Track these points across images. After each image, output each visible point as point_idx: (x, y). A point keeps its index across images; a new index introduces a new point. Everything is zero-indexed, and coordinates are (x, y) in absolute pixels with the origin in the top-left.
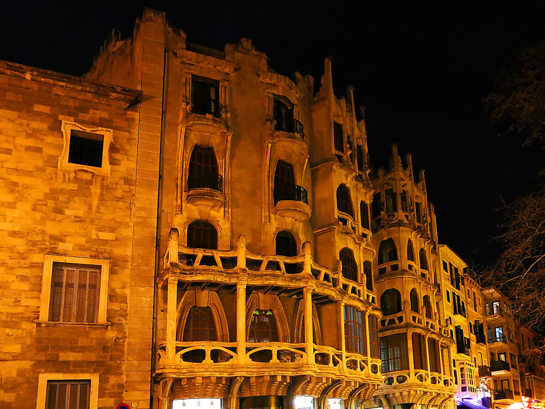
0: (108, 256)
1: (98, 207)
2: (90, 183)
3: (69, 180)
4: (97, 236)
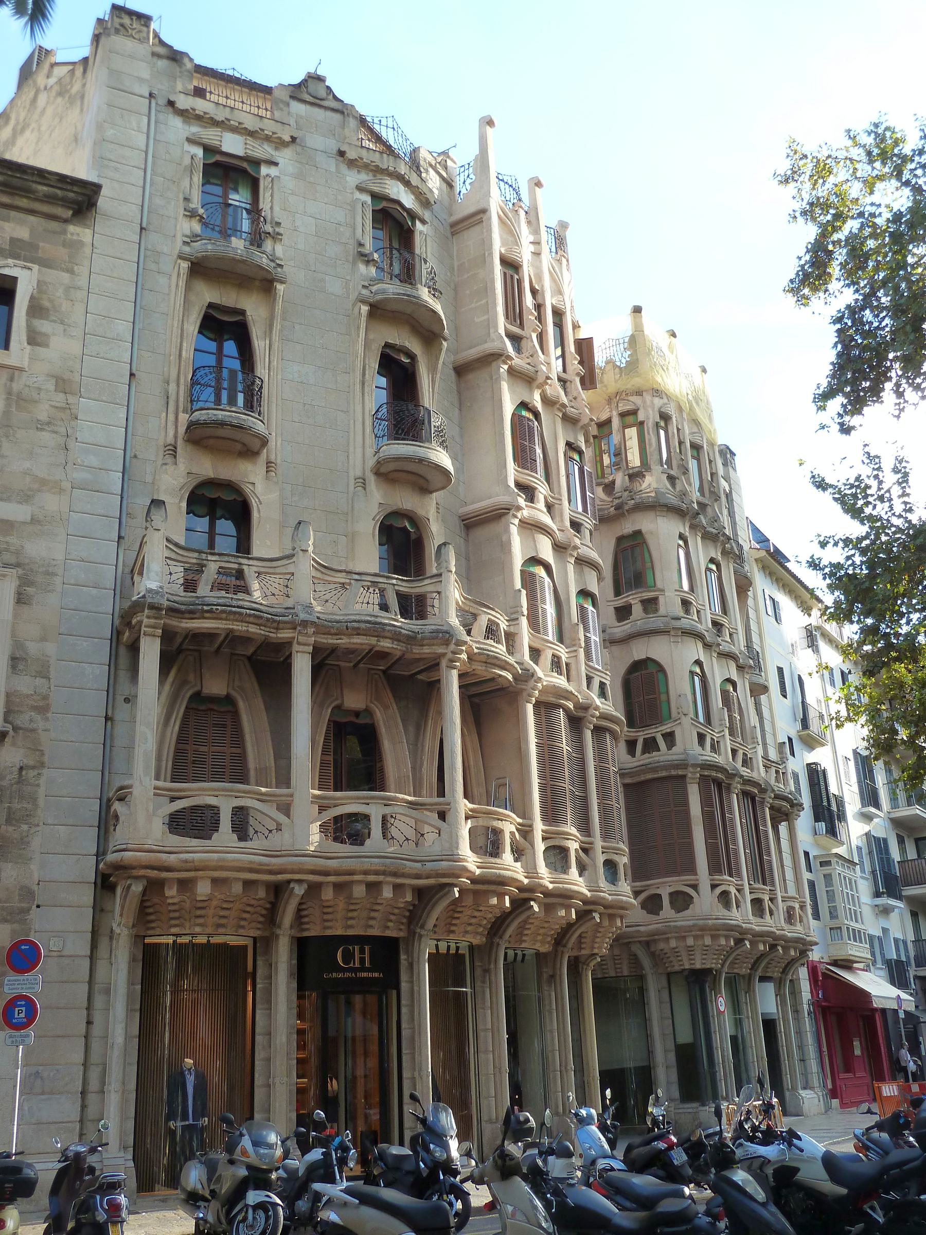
0: (13, 560)
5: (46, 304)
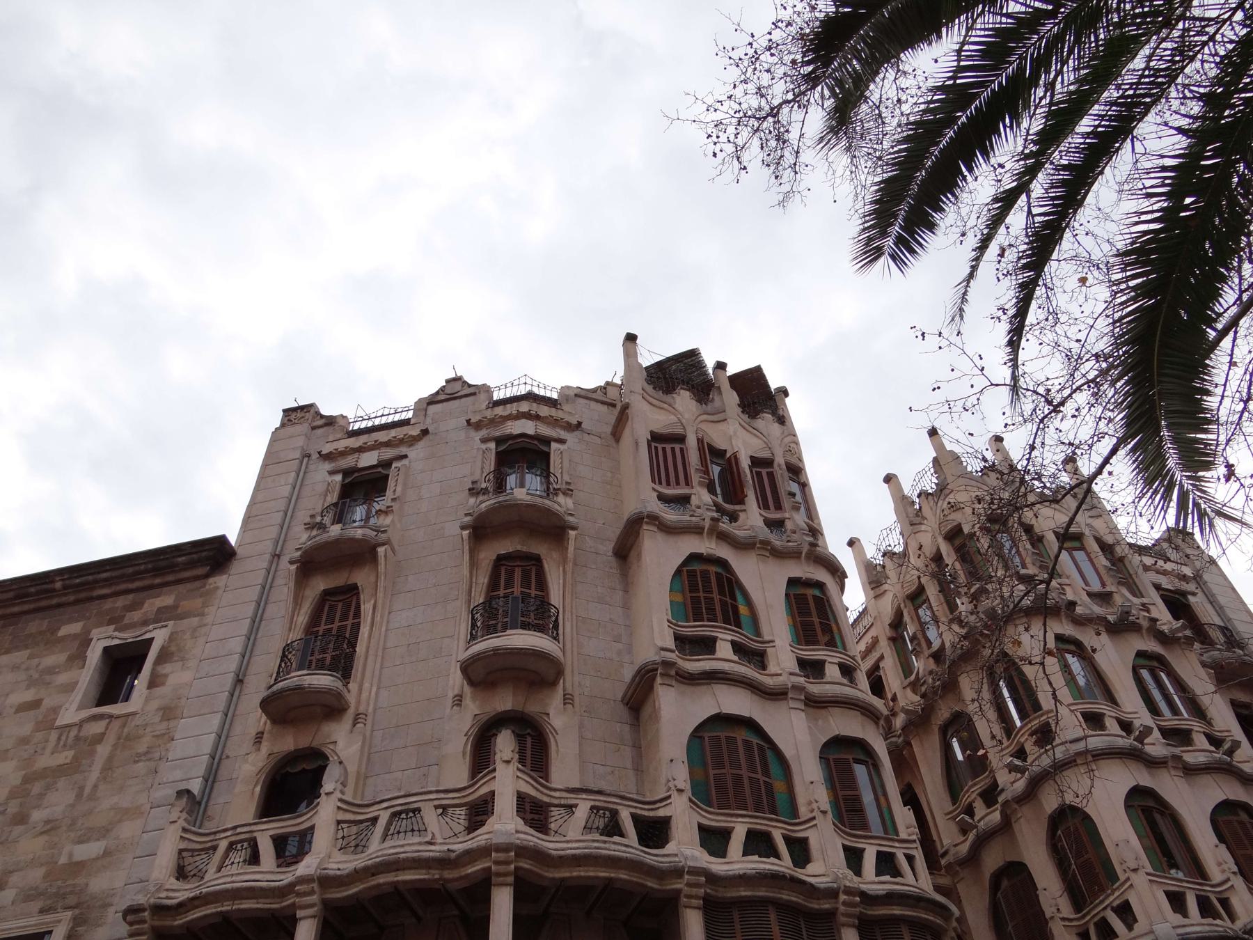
1: (95, 786)
2: (100, 738)
3: (65, 745)
4: (71, 855)
5: (173, 649)
